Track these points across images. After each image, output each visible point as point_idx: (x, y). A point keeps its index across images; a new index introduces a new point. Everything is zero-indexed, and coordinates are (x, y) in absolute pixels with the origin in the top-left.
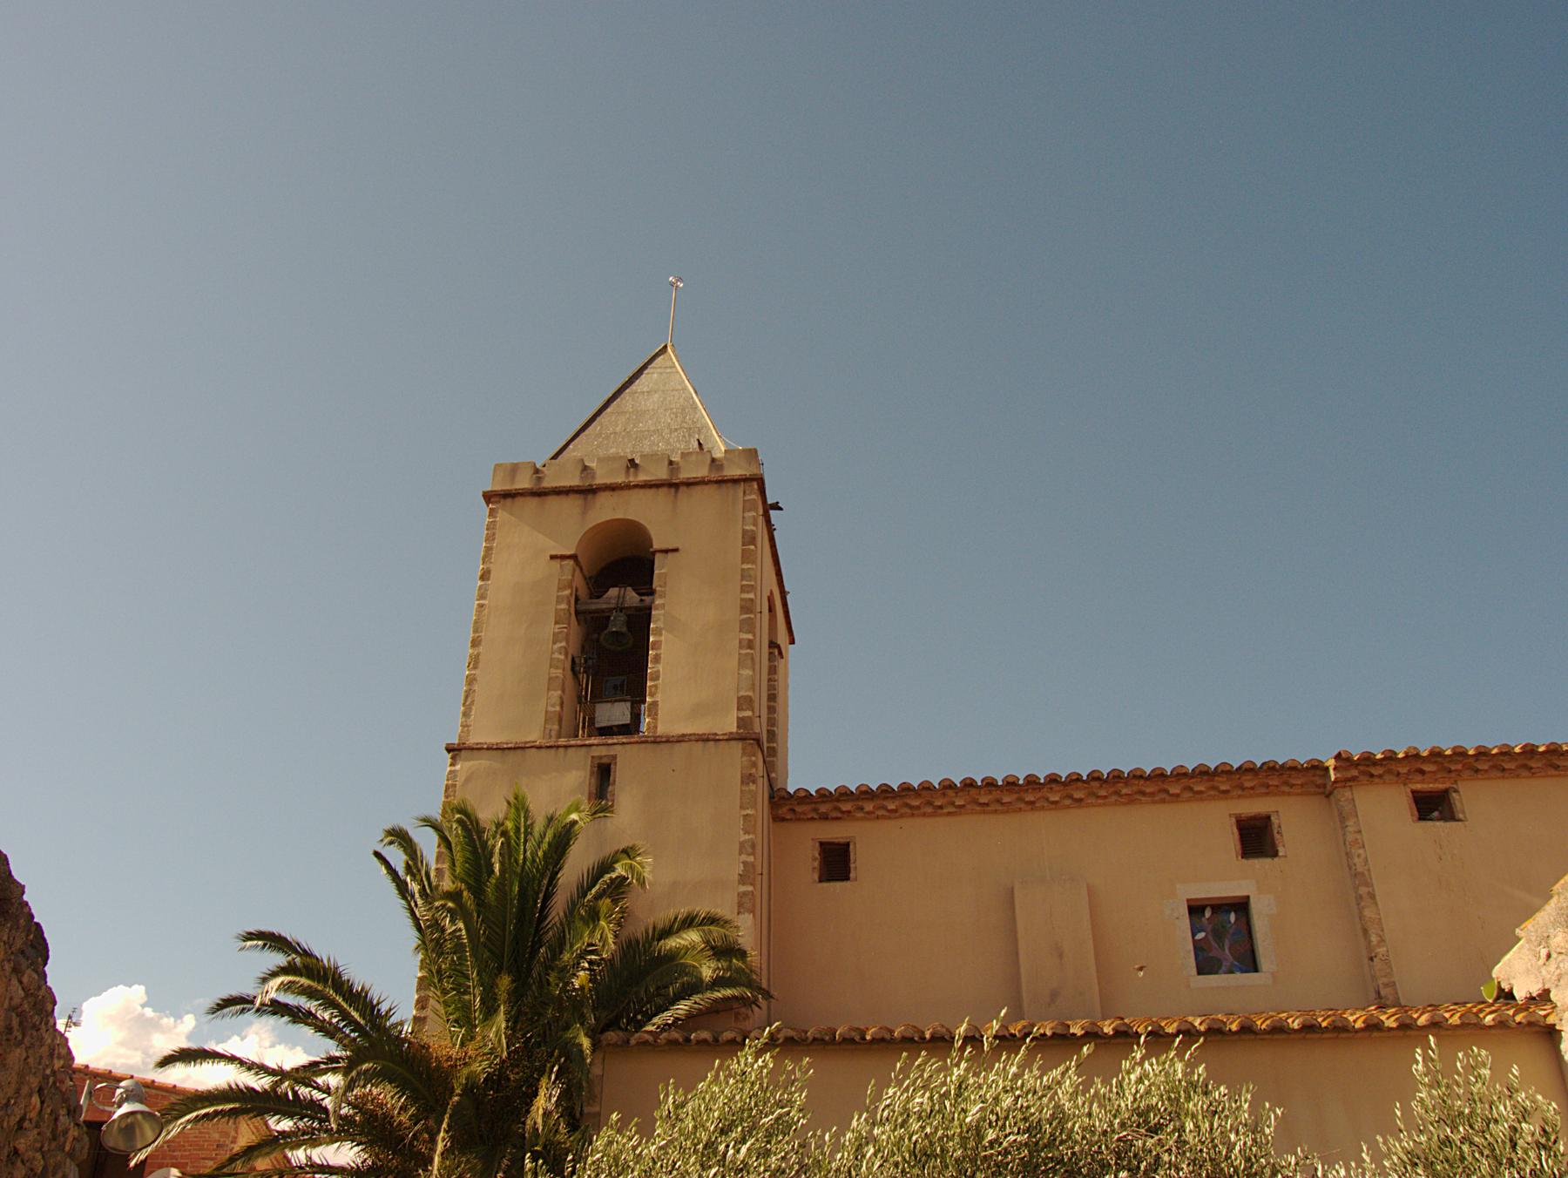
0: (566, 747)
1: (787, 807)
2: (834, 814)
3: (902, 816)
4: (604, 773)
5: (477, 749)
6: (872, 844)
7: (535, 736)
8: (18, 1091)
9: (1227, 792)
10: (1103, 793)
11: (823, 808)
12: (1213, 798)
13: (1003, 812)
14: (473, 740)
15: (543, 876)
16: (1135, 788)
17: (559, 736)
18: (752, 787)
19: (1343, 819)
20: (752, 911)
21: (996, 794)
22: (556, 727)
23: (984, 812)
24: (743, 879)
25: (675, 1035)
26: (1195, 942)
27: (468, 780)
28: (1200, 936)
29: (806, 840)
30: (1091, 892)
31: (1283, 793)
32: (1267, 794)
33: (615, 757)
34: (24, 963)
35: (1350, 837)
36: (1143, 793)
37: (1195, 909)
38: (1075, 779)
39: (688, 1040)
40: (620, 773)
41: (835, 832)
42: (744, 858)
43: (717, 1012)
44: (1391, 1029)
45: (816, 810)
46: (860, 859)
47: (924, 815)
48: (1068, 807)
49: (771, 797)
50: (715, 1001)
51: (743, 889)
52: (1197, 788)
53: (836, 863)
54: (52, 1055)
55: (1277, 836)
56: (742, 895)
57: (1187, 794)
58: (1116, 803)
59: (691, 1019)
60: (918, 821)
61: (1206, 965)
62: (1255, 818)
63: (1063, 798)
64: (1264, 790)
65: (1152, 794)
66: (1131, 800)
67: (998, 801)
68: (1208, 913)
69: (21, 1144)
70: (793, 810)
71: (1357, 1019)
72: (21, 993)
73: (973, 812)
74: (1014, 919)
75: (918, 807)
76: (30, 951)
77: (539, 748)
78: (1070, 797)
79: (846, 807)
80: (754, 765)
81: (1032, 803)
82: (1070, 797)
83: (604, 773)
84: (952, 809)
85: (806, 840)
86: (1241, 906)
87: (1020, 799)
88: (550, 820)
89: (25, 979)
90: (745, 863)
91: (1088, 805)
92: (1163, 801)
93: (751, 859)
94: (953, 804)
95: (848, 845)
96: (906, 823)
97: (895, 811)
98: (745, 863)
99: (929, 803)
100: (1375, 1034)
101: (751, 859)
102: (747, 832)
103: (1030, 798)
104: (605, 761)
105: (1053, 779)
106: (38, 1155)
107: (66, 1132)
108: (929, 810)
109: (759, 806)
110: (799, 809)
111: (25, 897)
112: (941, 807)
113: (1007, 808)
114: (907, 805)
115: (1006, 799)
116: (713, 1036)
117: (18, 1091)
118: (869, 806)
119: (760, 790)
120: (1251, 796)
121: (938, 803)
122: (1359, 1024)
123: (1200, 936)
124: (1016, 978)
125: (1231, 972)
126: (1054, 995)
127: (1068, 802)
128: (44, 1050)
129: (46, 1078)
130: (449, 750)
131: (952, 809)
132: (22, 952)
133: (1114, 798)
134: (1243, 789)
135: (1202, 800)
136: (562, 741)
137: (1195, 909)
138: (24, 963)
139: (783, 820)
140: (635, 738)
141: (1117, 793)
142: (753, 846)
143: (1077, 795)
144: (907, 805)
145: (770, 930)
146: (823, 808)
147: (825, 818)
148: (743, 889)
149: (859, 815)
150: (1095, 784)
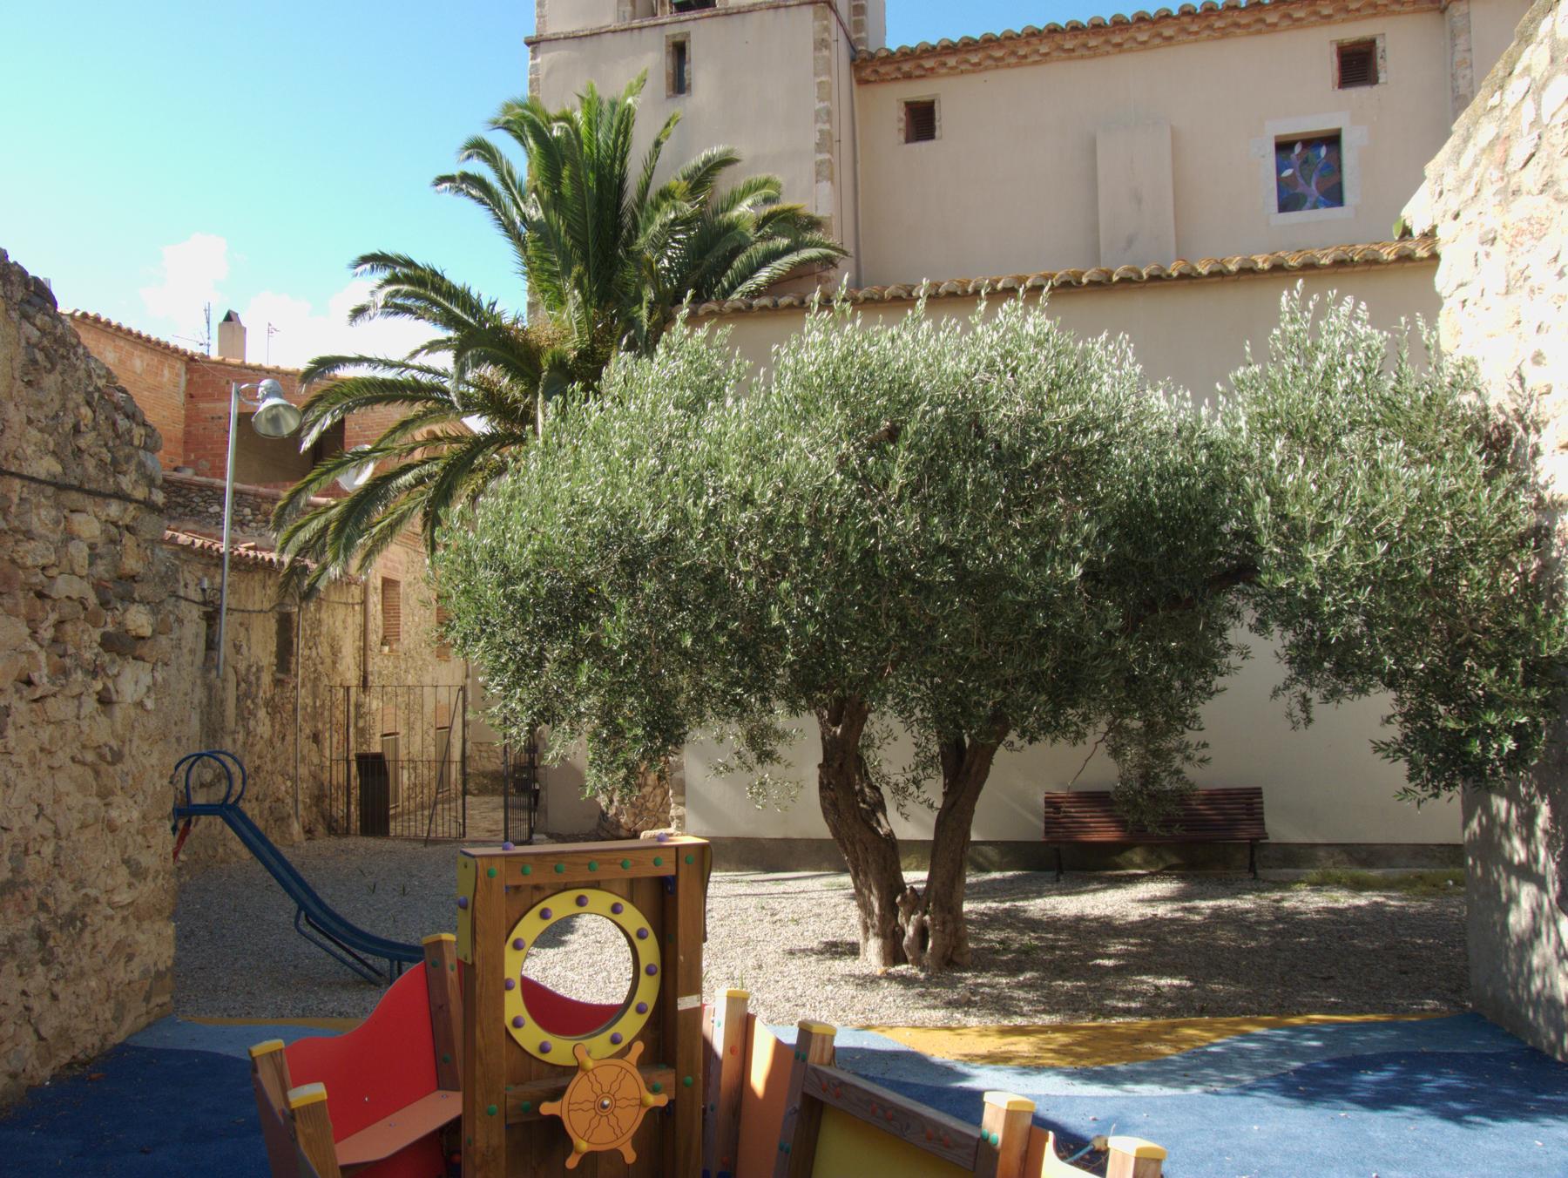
0: (640, 28)
1: (869, 66)
2: (918, 73)
3: (986, 69)
4: (679, 51)
5: (555, 39)
6: (955, 98)
7: (609, 20)
8: (64, 406)
9: (1329, 16)
10: (1194, 28)
11: (906, 67)
12: (1313, 25)
13: (1090, 57)
14: (551, 30)
15: (613, 161)
16: (1229, 21)
17: (634, 17)
18: (826, 53)
19: (1454, 37)
20: (831, 179)
21: (1082, 38)
22: (629, 8)
23: (1070, 59)
24: (820, 148)
25: (765, 301)
26: (1279, 180)
27: (549, 73)
28: (1287, 173)
29: (892, 100)
30: (1175, 135)
31: (1393, 13)
32: (1374, 15)
33: (688, 35)
34: (30, 310)
35: (1458, 57)
36: (1237, 25)
37: (1284, 146)
38: (1165, 16)
39: (776, 305)
40: (694, 51)
41: (919, 91)
42: (820, 126)
43: (800, 277)
44: (1422, 259)
45: (899, 69)
46: (945, 118)
47: (1008, 66)
48: (1158, 46)
49: (853, 60)
50: (793, 264)
51: (820, 157)
52: (1296, 15)
53: (921, 121)
54: (90, 376)
55: (1379, 61)
56: (819, 164)
57: (1286, 23)
58: (1209, 38)
59: (774, 285)
60: (1004, 74)
61: (1288, 201)
62: (1358, 43)
63: (1152, 37)
64: (1371, 11)
65: (1248, 26)
66: (1224, 34)
67: (1085, 46)
68: (1298, 149)
69: (82, 443)
70: (876, 72)
71: (1388, 254)
72: (38, 333)
73: (1059, 59)
74: (1094, 168)
75: (1002, 59)
76: (36, 300)
77: (614, 32)
78: (1159, 35)
79: (928, 64)
80: (826, 29)
81: (1119, 45)
82: (1159, 35)
83: (679, 51)
84: (1037, 58)
85: (892, 100)
86: (1333, 140)
87: (1107, 42)
88: (613, 105)
89: (38, 322)
90: (821, 131)
91: (1179, 43)
92: (1259, 32)
93: (826, 127)
94: (1037, 52)
95: (932, 103)
96: (991, 76)
97: (979, 64)
98: (821, 131)
99: (1014, 53)
100: (1408, 265)
101: (826, 127)
102: (821, 100)
103: (1117, 39)
104: (679, 39)
105: (1141, 19)
106: (104, 450)
107: (129, 431)
108: (1013, 60)
109: (834, 73)
110: (882, 70)
111: (11, 260)
112: (1025, 57)
113: (1094, 53)
114: (990, 57)
115: (1092, 43)
116: (787, 299)
117: (64, 406)
118: (952, 61)
119: (840, 55)
120: (1356, 19)
121: (1021, 52)
122: (1392, 257)
123: (1287, 173)
124: (1094, 228)
125: (1315, 207)
126: (1130, 241)
127: (1158, 41)
128: (81, 374)
129: (90, 394)
130: (529, 43)
131: (1037, 58)
132: (29, 302)
133: (1207, 33)
134: (1348, 11)
135: (1302, 27)
136: (636, 23)
137: (1284, 146)
138: (30, 310)
139: (867, 82)
140: (707, 12)
141: (1210, 27)
142: (829, 113)
143: (1167, 32)
144: (990, 57)
145: (858, 194)
146: (906, 67)
147: (908, 76)
148: (820, 157)
149: (944, 71)
150: (1186, 19)
